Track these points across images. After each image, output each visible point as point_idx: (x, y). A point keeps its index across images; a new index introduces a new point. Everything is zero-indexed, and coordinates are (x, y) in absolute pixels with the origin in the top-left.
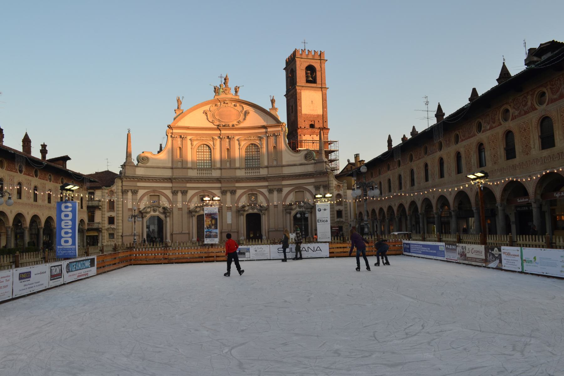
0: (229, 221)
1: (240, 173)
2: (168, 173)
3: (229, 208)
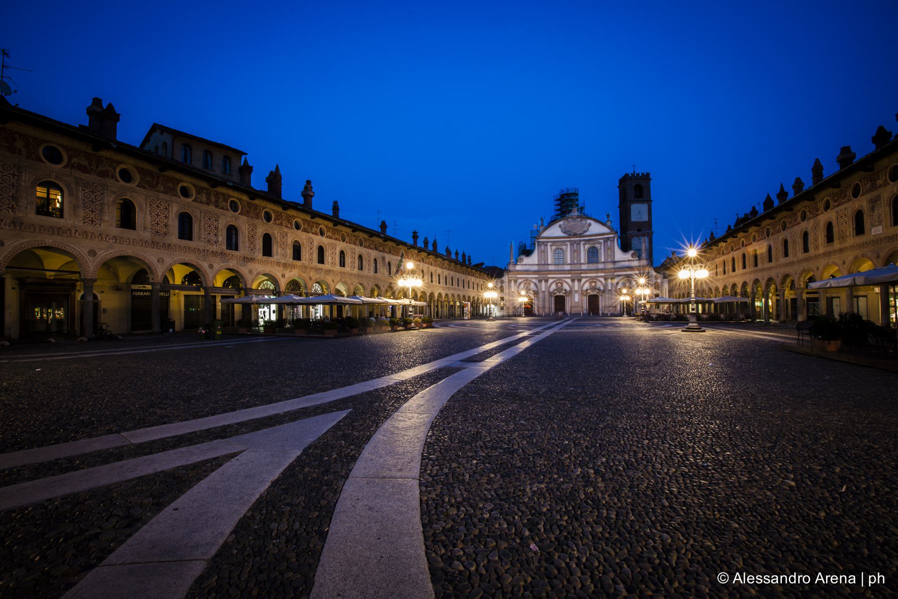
0: (577, 300)
1: (584, 267)
2: (536, 268)
3: (576, 291)
